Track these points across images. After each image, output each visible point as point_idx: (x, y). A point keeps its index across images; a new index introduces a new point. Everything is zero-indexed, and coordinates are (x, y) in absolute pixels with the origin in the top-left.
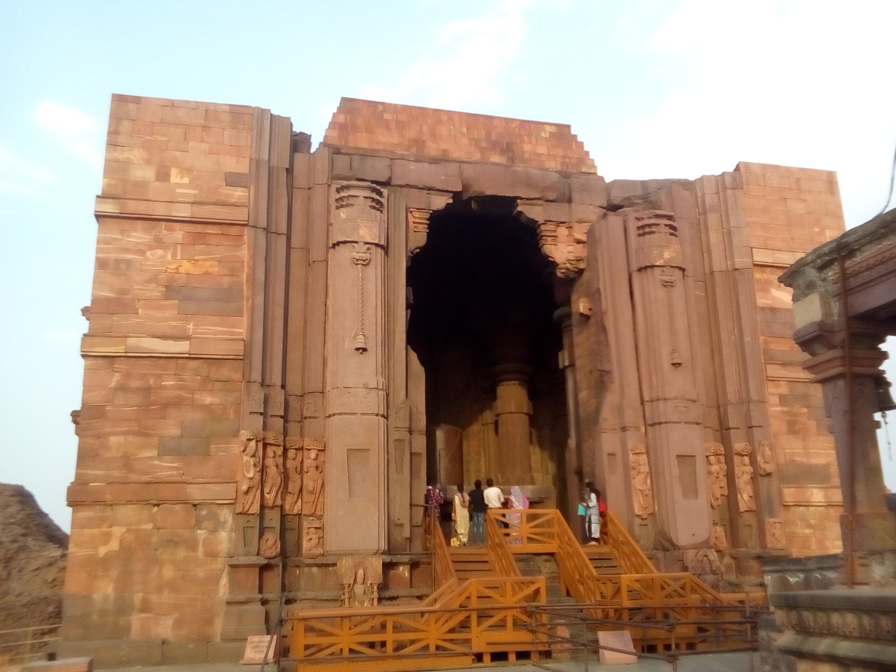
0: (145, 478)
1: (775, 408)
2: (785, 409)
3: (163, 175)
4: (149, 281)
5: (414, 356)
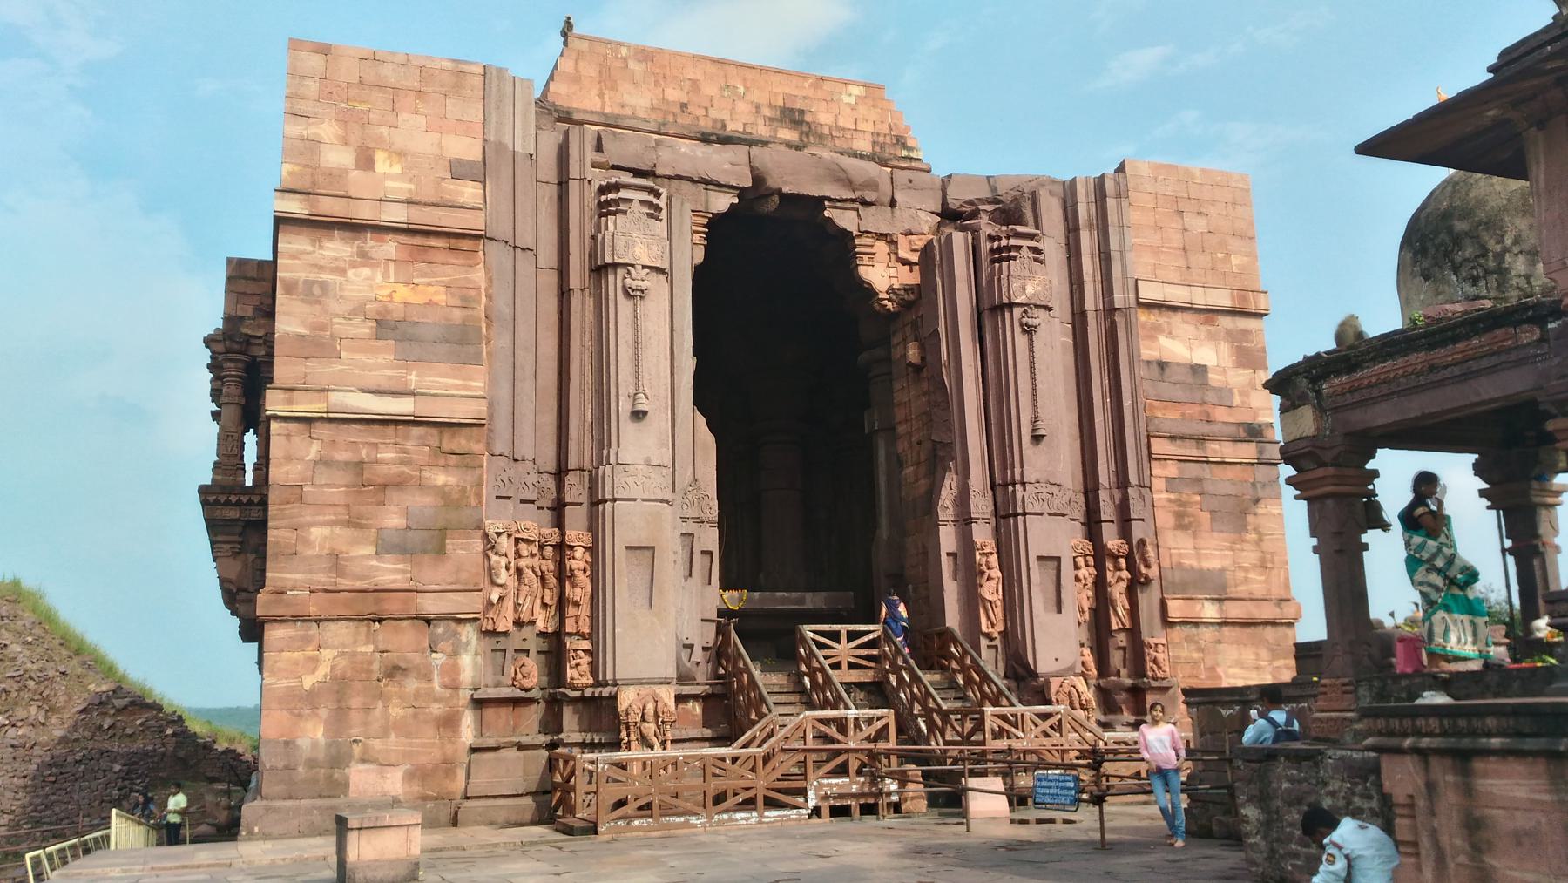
0: (358, 585)
1: (1161, 497)
2: (1172, 496)
3: (366, 161)
4: (354, 313)
5: (701, 420)
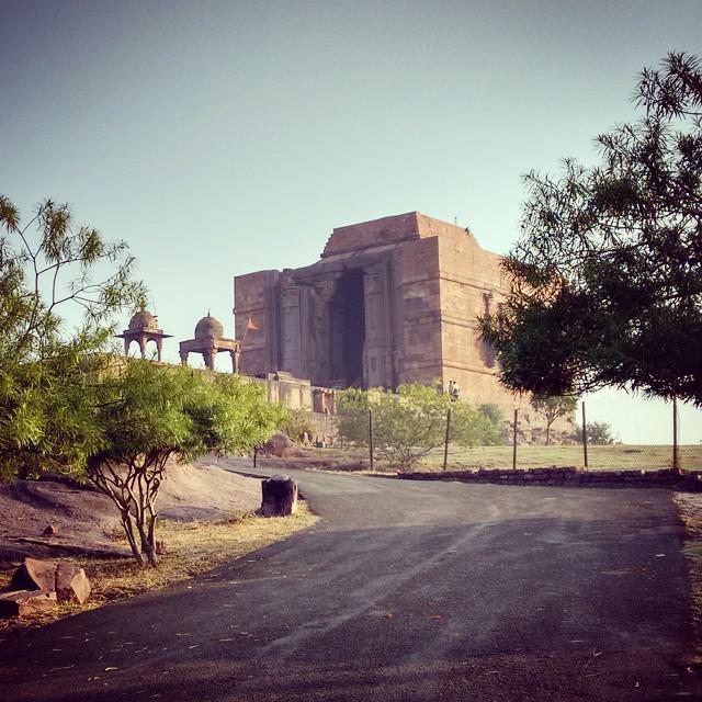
1: (406, 337)
